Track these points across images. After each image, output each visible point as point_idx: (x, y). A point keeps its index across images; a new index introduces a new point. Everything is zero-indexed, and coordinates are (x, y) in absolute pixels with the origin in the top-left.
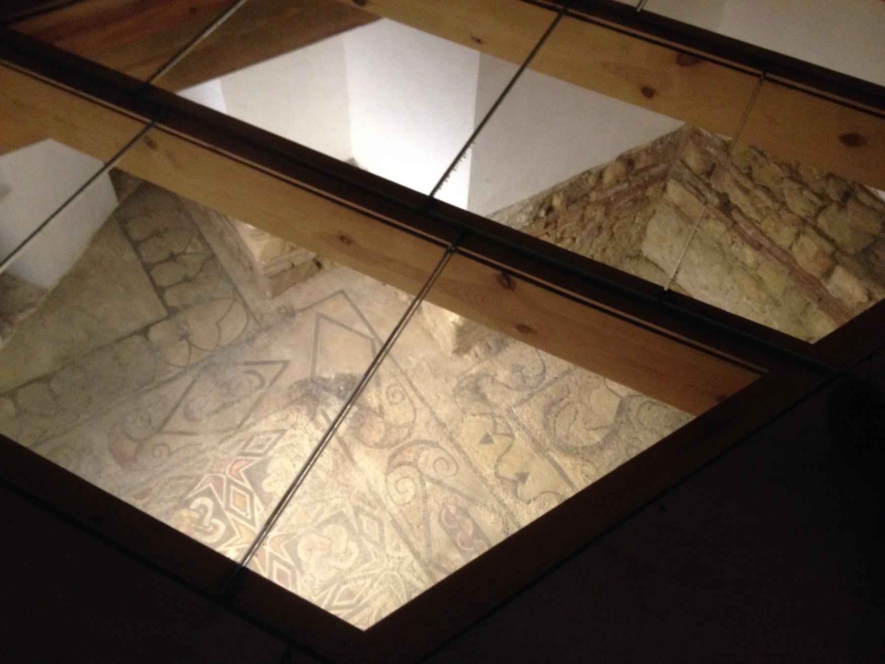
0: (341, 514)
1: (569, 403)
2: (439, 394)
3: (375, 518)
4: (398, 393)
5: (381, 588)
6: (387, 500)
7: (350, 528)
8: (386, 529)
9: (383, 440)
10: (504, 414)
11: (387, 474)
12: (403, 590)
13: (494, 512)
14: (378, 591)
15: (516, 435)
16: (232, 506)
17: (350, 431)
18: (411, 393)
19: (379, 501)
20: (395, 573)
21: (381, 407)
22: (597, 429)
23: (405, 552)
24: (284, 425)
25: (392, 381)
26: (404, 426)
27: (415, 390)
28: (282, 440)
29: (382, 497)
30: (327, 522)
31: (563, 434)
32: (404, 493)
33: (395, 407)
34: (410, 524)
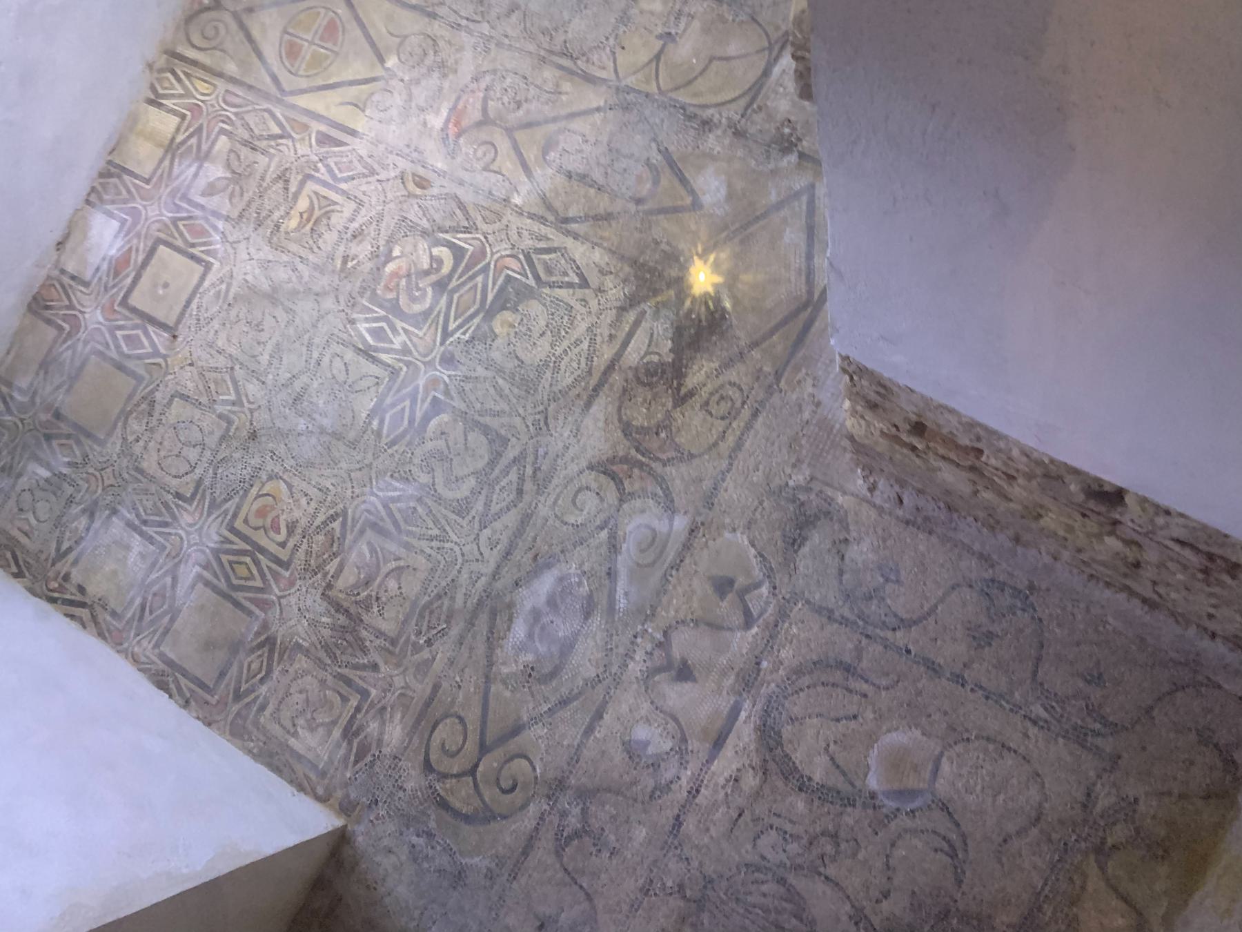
0: (505, 442)
1: (865, 696)
3: (520, 492)
4: (729, 404)
5: (433, 553)
6: (554, 489)
7: (492, 463)
8: (514, 511)
9: (642, 430)
10: (784, 591)
11: (591, 467)
12: (444, 584)
13: (606, 655)
14: (428, 551)
15: (755, 630)
16: (456, 296)
17: (630, 375)
19: (548, 479)
20: (460, 560)
21: (691, 394)
22: (838, 767)
23: (493, 557)
24: (594, 280)
25: (745, 381)
26: (678, 448)
27: (748, 426)
28: (571, 291)
29: (555, 481)
30: (486, 430)
31: (796, 711)
32: (577, 508)
33: (702, 414)
34: (535, 539)
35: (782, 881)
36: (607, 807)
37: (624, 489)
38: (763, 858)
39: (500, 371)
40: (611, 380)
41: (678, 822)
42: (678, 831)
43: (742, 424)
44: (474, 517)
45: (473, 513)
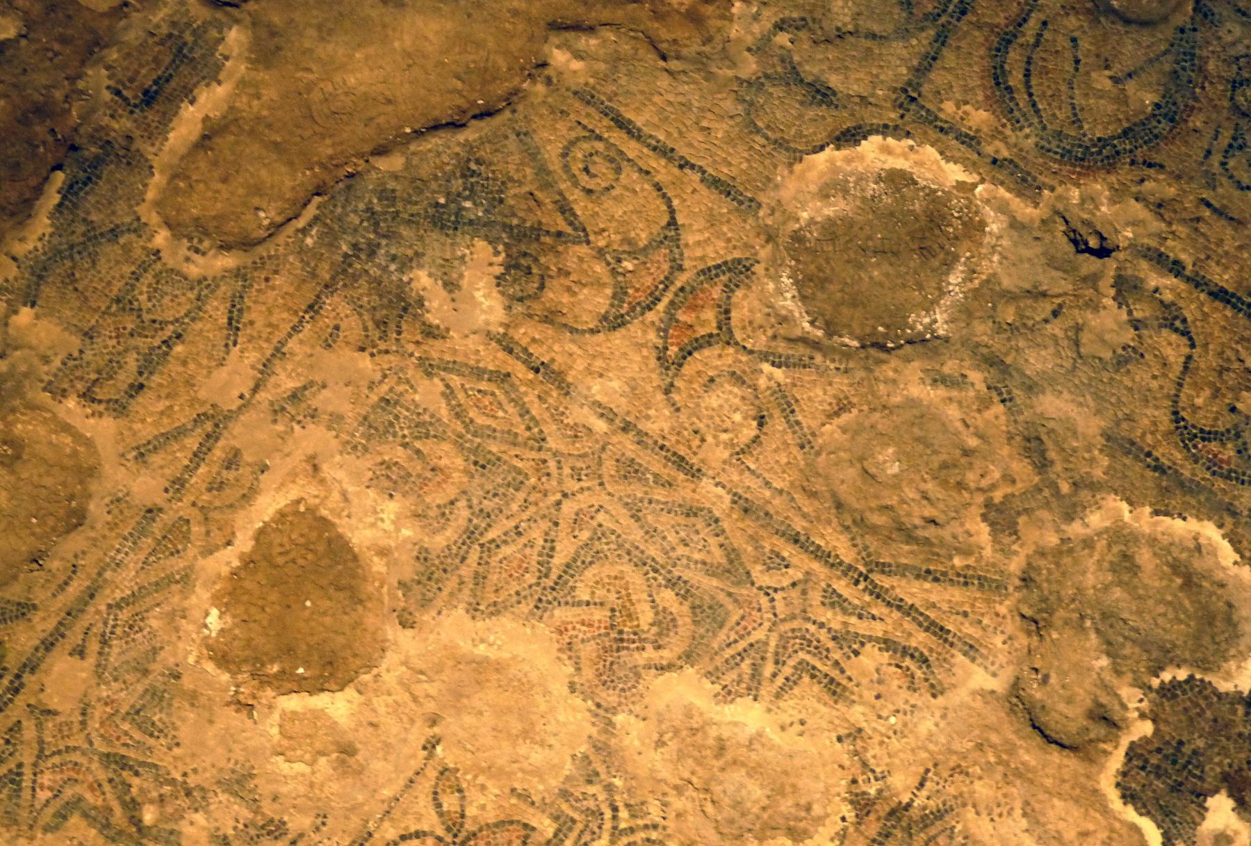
0: (599, 534)
2: (704, 124)
17: (519, 308)
18: (632, 149)
23: (802, 564)
33: (608, 203)
36: (1199, 401)
37: (711, 335)
39: (471, 534)
40: (524, 342)
41: (1220, 295)
42: (1233, 295)
43: (633, 144)
44: (730, 594)
45: (722, 597)
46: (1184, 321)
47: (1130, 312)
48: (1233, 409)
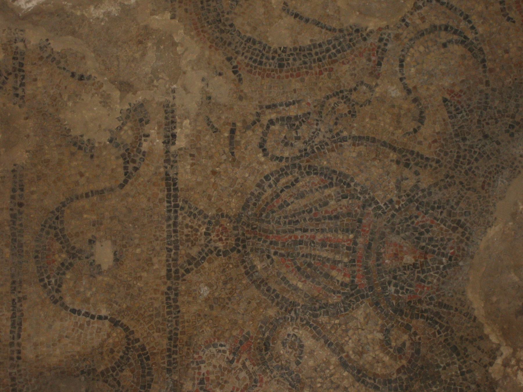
22: (307, 21)
35: (311, 170)
38: (280, 159)
46: (136, 169)
47: (120, 128)
48: (91, 242)
